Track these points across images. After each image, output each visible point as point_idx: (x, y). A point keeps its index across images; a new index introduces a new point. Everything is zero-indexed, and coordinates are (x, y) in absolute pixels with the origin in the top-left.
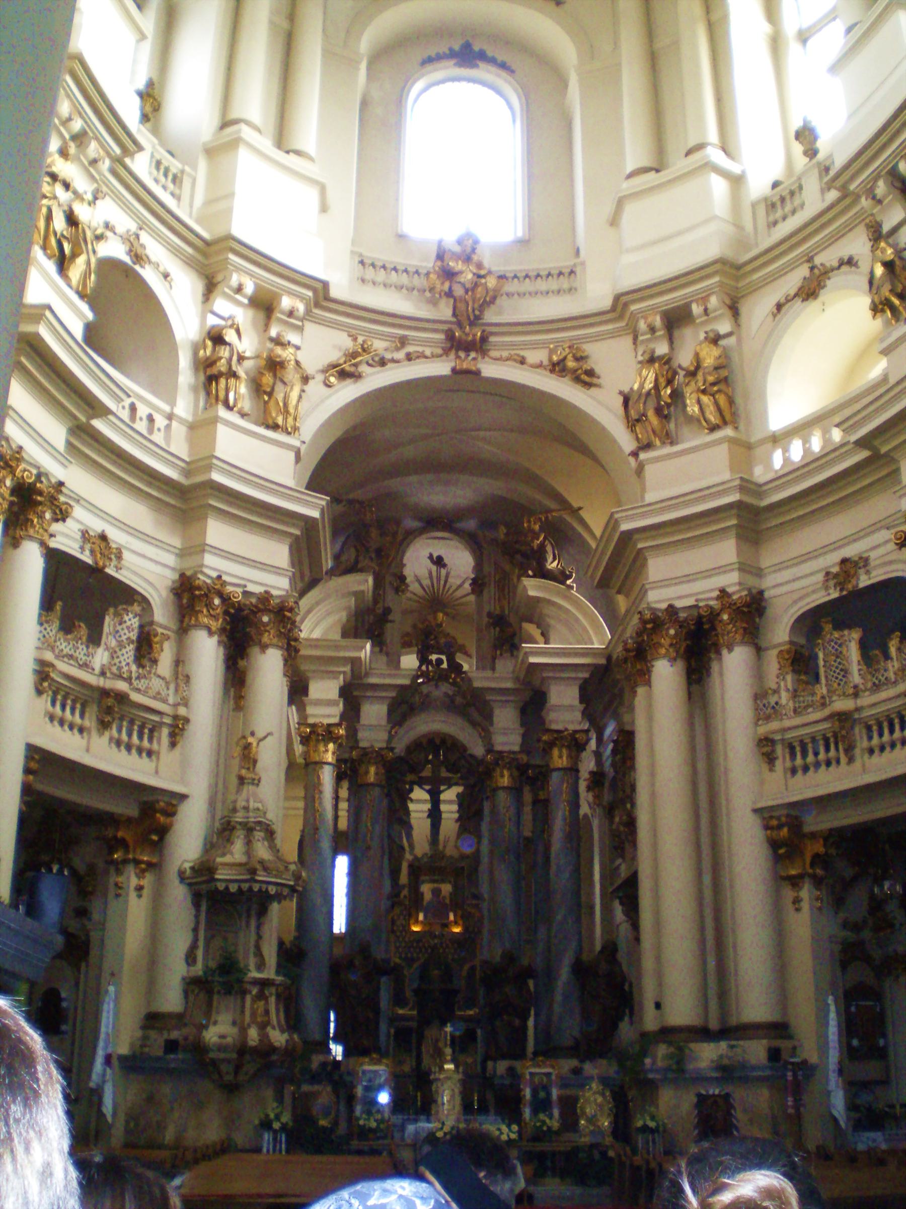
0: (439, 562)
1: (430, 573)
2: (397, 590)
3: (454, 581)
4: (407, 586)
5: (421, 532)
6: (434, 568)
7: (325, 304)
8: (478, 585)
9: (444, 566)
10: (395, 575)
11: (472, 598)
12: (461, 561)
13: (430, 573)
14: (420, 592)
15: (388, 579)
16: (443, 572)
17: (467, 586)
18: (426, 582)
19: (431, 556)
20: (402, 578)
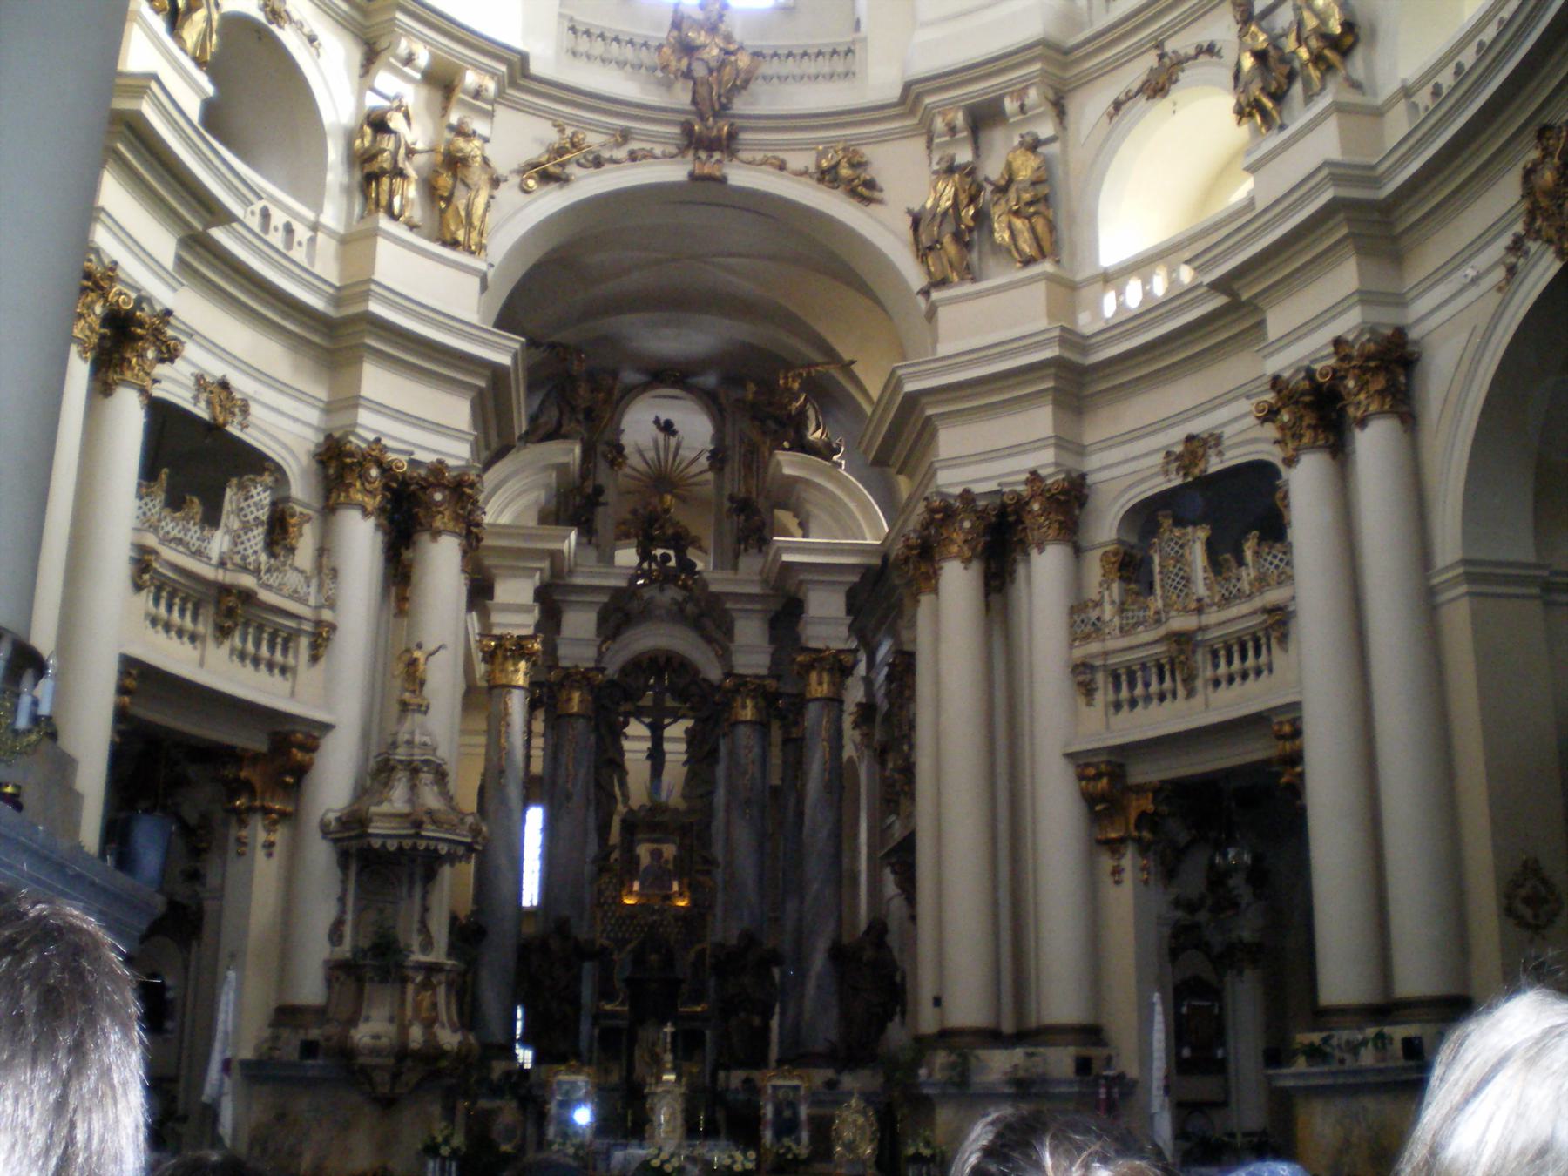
0: (667, 428)
1: (656, 442)
3: (687, 454)
4: (625, 458)
6: (661, 436)
7: (522, 82)
8: (718, 458)
9: (674, 433)
10: (607, 443)
11: (710, 476)
12: (696, 429)
14: (642, 466)
15: (601, 448)
16: (673, 441)
17: (704, 462)
18: (651, 455)
19: (657, 421)
20: (619, 449)
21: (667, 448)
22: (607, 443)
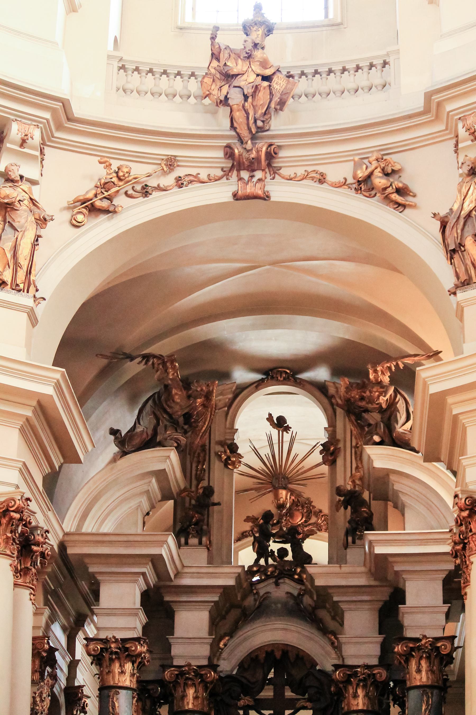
0: (280, 424)
1: (270, 439)
2: (226, 464)
3: (300, 449)
4: (240, 456)
5: (258, 385)
6: (275, 432)
8: (330, 452)
9: (287, 429)
10: (222, 443)
11: (325, 469)
13: (270, 439)
14: (258, 465)
16: (287, 437)
17: (317, 457)
18: (265, 452)
19: (270, 418)
20: (233, 448)
21: (281, 442)
22: (222, 443)
